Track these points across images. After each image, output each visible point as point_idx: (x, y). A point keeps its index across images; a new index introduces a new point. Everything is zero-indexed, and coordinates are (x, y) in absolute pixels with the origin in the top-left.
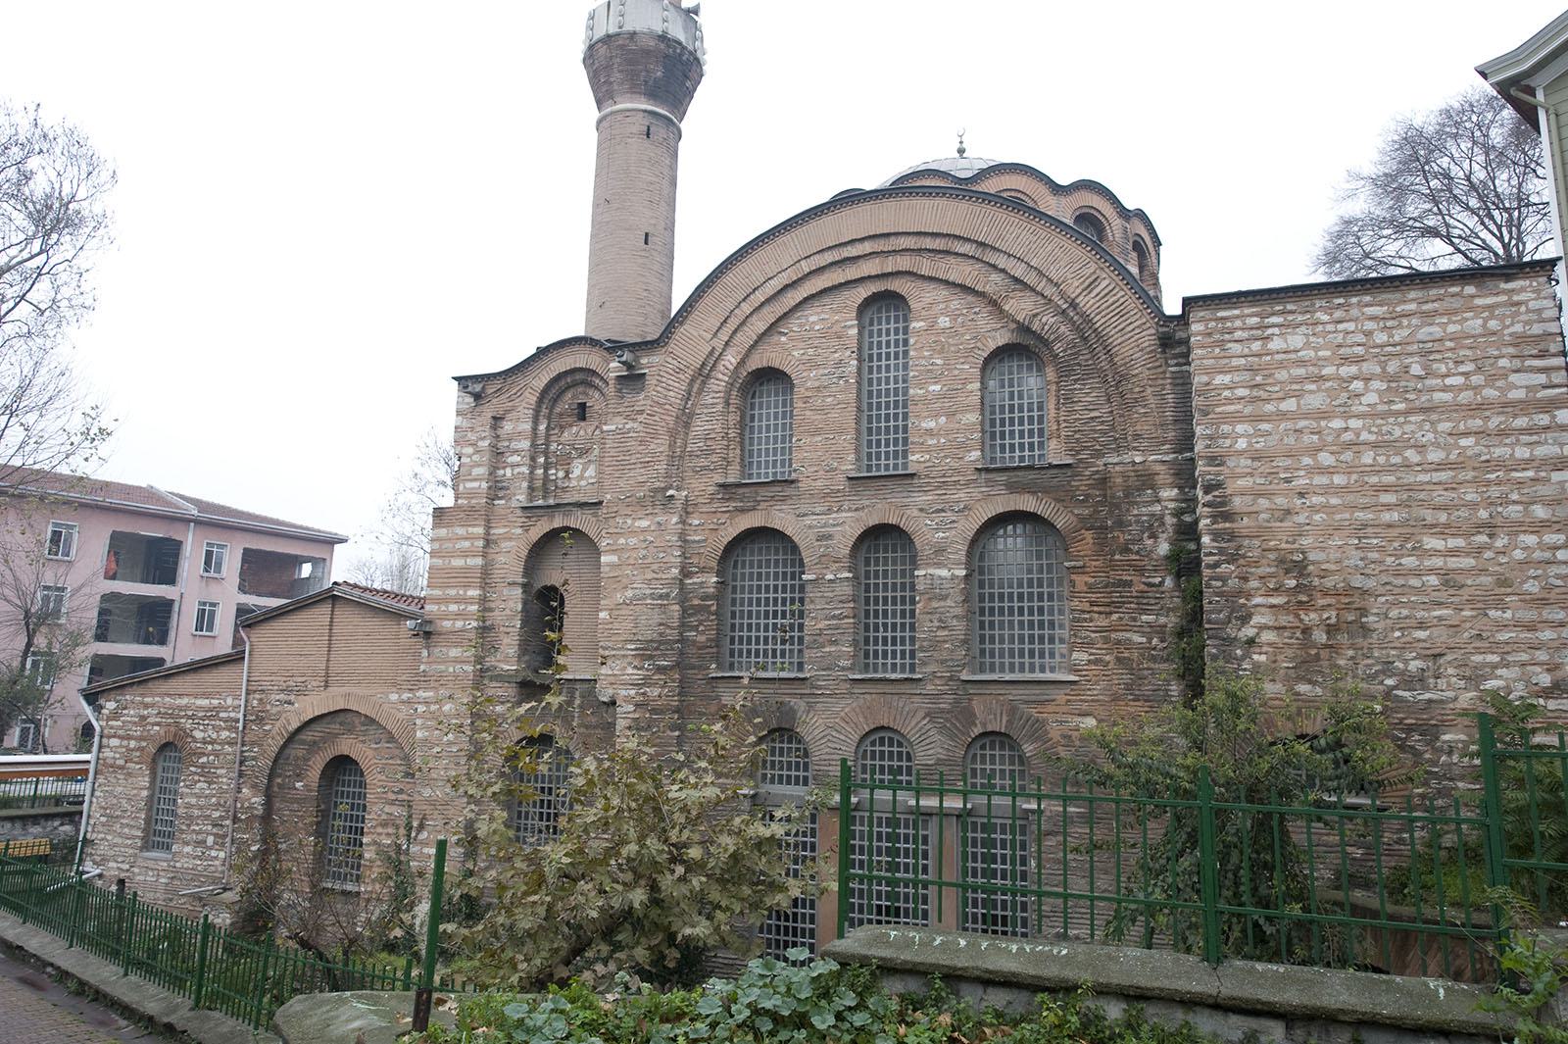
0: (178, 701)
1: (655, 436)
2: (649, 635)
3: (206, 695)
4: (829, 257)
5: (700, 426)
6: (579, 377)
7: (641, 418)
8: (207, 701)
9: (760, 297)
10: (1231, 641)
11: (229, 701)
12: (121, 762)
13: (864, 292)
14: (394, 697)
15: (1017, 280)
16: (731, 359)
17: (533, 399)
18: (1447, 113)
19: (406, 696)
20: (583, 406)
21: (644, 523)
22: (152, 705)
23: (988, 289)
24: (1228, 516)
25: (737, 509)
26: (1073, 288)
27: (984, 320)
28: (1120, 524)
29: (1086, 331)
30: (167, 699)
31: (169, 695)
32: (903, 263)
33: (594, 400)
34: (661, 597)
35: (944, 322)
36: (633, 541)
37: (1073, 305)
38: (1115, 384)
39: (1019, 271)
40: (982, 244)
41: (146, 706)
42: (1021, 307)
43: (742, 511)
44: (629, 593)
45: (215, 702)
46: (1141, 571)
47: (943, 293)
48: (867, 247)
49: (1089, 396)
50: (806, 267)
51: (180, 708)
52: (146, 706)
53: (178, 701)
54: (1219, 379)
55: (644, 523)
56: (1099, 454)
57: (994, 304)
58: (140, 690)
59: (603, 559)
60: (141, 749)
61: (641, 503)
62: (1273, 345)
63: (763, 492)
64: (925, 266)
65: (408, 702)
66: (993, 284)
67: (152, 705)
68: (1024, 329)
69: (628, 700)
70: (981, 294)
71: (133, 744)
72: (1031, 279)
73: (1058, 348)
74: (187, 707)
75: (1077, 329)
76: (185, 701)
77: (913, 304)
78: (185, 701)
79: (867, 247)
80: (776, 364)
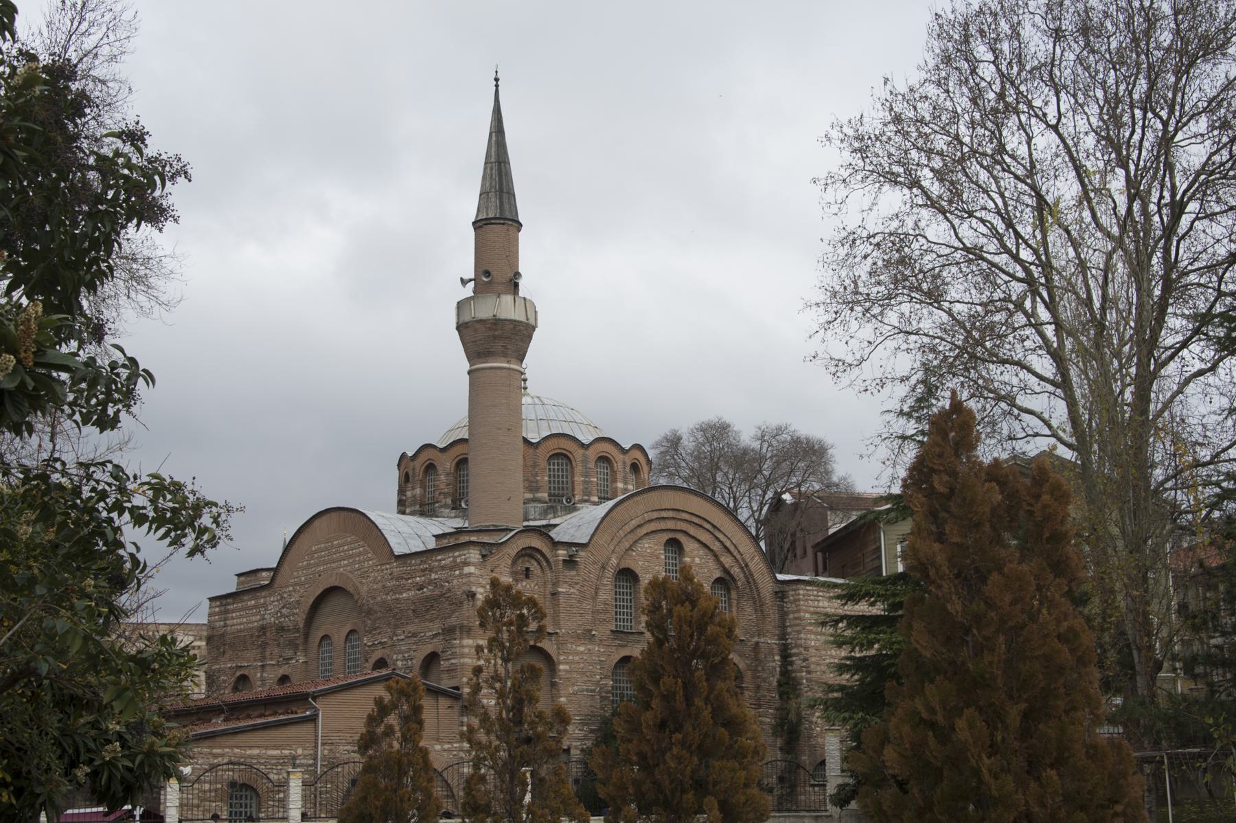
0: (249, 752)
1: (585, 599)
2: (586, 711)
3: (276, 747)
4: (655, 515)
5: (602, 596)
6: (529, 552)
7: (578, 587)
8: (278, 752)
9: (627, 528)
10: (811, 722)
11: (300, 751)
12: (196, 802)
13: (666, 536)
14: (438, 747)
15: (725, 547)
16: (614, 561)
17: (510, 562)
18: (717, 432)
19: (446, 746)
20: (527, 569)
21: (582, 649)
22: (222, 755)
23: (715, 548)
24: (809, 672)
25: (620, 646)
26: (747, 557)
27: (712, 563)
28: (763, 670)
29: (749, 576)
30: (237, 750)
31: (238, 747)
32: (684, 526)
33: (534, 566)
34: (592, 691)
35: (697, 560)
36: (577, 658)
37: (747, 565)
38: (759, 606)
39: (728, 544)
40: (714, 527)
41: (216, 756)
42: (727, 560)
43: (620, 646)
44: (576, 688)
45: (286, 752)
46: (769, 690)
47: (697, 545)
48: (671, 514)
49: (749, 608)
50: (647, 517)
51: (251, 757)
52: (216, 756)
53: (249, 752)
54: (807, 615)
55: (582, 649)
56: (752, 636)
57: (716, 556)
58: (207, 743)
59: (562, 667)
60: (216, 790)
61: (578, 637)
62: (821, 604)
63: (631, 637)
64: (692, 530)
65: (448, 750)
66: (716, 547)
67: (222, 755)
68: (726, 571)
69: (576, 748)
70: (711, 550)
71: (207, 786)
72: (732, 548)
73: (739, 584)
74: (259, 756)
75: (746, 577)
76: (256, 752)
77: (686, 549)
78: (256, 752)
79: (671, 514)
80: (632, 567)
